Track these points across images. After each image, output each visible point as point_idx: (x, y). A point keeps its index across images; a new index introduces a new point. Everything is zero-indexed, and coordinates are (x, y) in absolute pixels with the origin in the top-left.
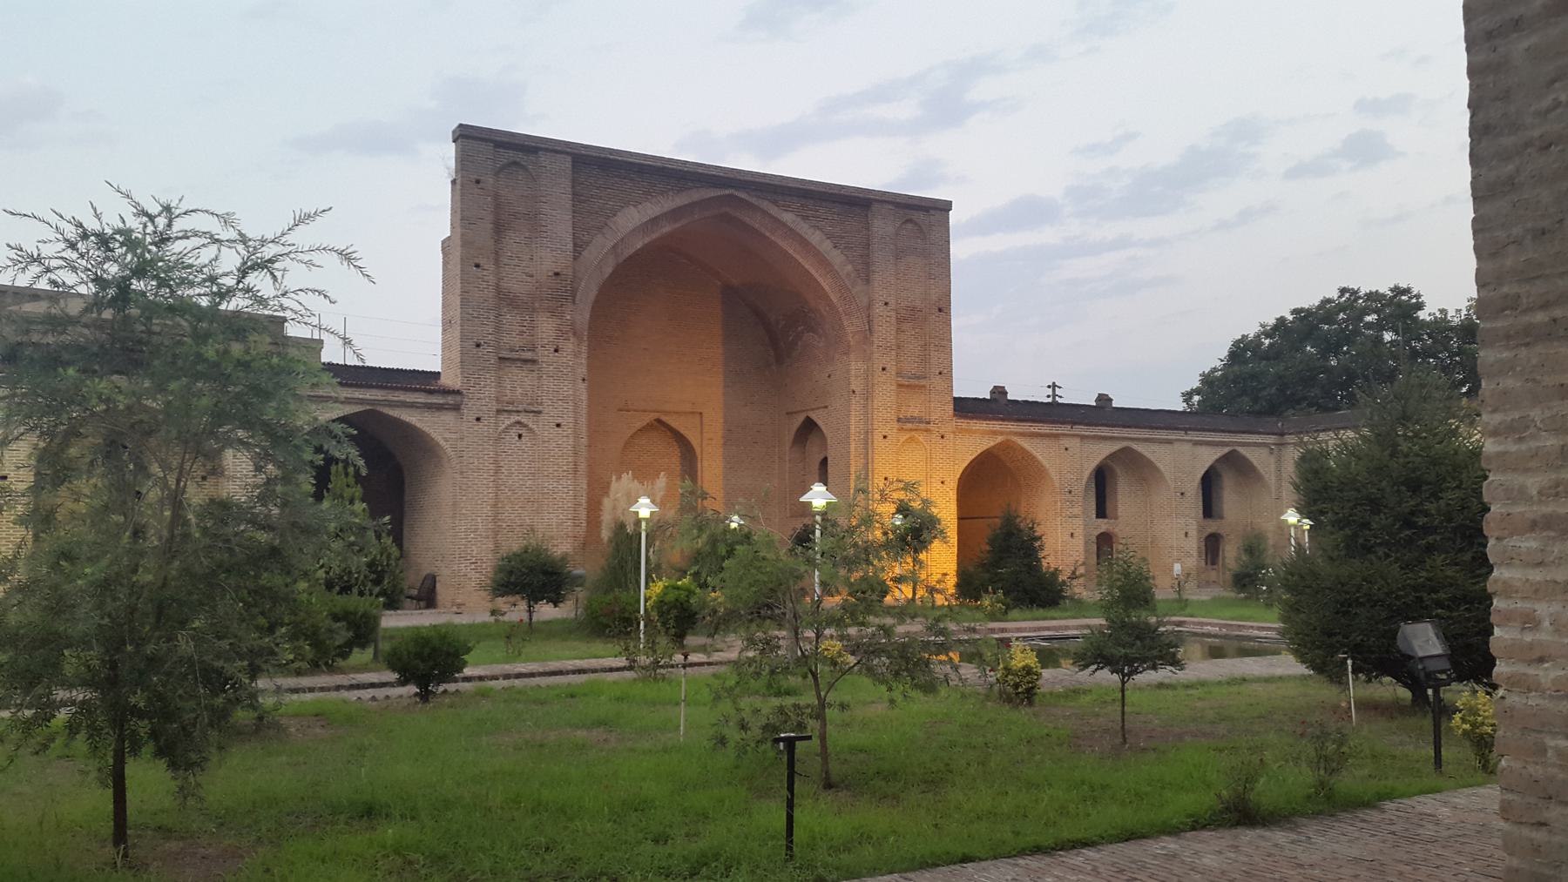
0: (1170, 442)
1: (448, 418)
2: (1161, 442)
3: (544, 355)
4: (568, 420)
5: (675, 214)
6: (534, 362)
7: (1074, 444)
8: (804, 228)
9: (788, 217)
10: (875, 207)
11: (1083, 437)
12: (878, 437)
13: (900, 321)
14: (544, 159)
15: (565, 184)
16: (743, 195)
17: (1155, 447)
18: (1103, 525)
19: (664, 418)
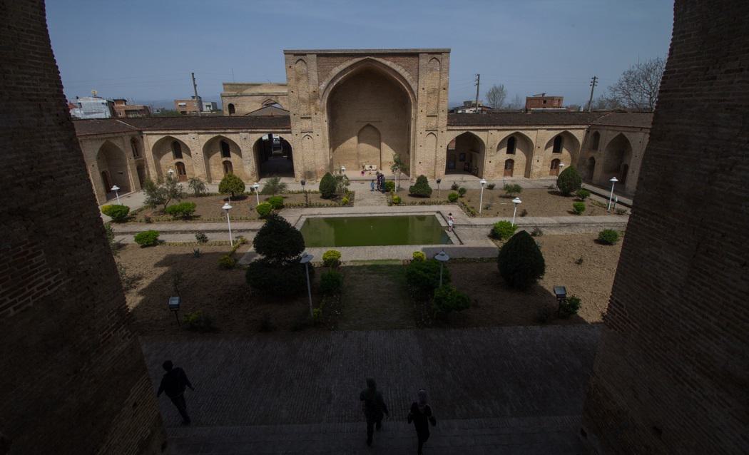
0: (537, 129)
1: (289, 135)
2: (532, 130)
3: (313, 116)
4: (320, 134)
5: (351, 67)
6: (310, 118)
7: (495, 132)
8: (394, 66)
9: (388, 63)
10: (420, 55)
11: (498, 130)
12: (418, 133)
13: (429, 93)
14: (308, 56)
15: (315, 62)
16: (373, 58)
17: (528, 131)
18: (509, 156)
19: (373, 124)
